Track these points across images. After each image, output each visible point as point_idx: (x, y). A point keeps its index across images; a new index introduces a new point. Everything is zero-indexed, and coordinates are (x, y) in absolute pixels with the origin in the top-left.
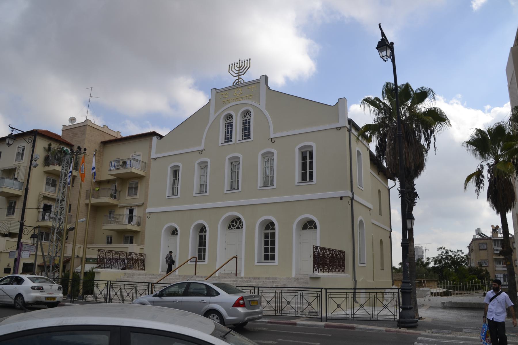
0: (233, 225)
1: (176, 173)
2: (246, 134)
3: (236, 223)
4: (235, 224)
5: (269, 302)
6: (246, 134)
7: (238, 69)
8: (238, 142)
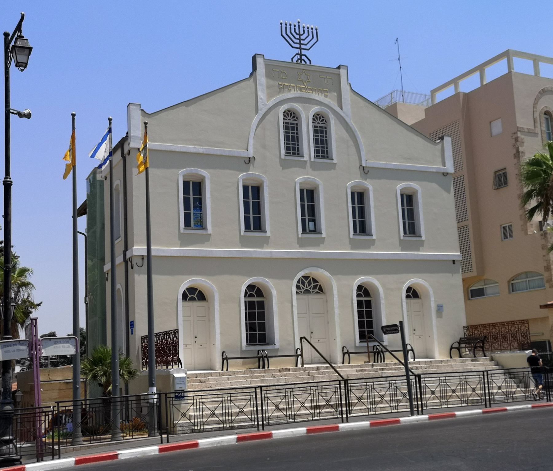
5: (474, 390)
7: (297, 37)
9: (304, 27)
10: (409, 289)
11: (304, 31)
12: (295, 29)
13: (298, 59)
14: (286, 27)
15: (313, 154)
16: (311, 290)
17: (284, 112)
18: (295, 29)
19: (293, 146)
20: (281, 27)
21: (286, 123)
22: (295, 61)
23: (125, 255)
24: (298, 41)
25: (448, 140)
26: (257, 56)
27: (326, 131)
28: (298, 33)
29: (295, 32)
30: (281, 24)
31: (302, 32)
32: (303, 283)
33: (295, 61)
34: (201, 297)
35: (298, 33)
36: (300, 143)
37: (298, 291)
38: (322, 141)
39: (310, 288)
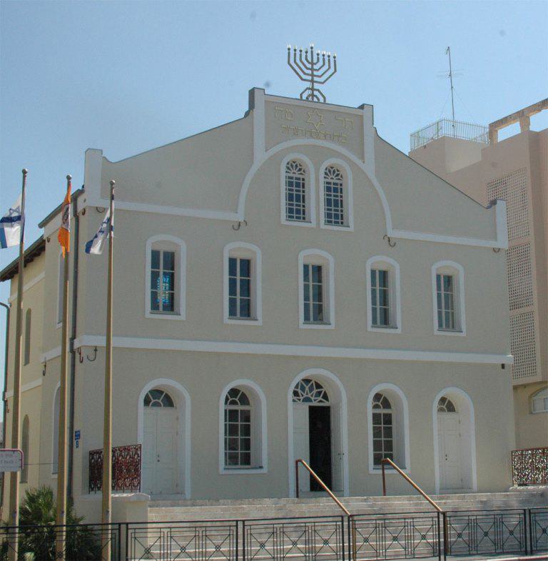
2: (335, 213)
6: (335, 213)
7: (309, 66)
9: (318, 54)
10: (443, 400)
11: (318, 58)
12: (306, 56)
13: (309, 96)
14: (295, 54)
15: (323, 218)
16: (313, 398)
17: (288, 163)
18: (306, 56)
19: (296, 207)
20: (289, 53)
21: (290, 178)
22: (304, 98)
23: (72, 345)
24: (310, 72)
25: (501, 205)
26: (256, 90)
27: (341, 189)
28: (310, 61)
29: (306, 59)
30: (289, 49)
31: (315, 61)
32: (303, 389)
33: (304, 98)
34: (169, 402)
35: (310, 60)
36: (306, 204)
37: (295, 398)
38: (336, 202)
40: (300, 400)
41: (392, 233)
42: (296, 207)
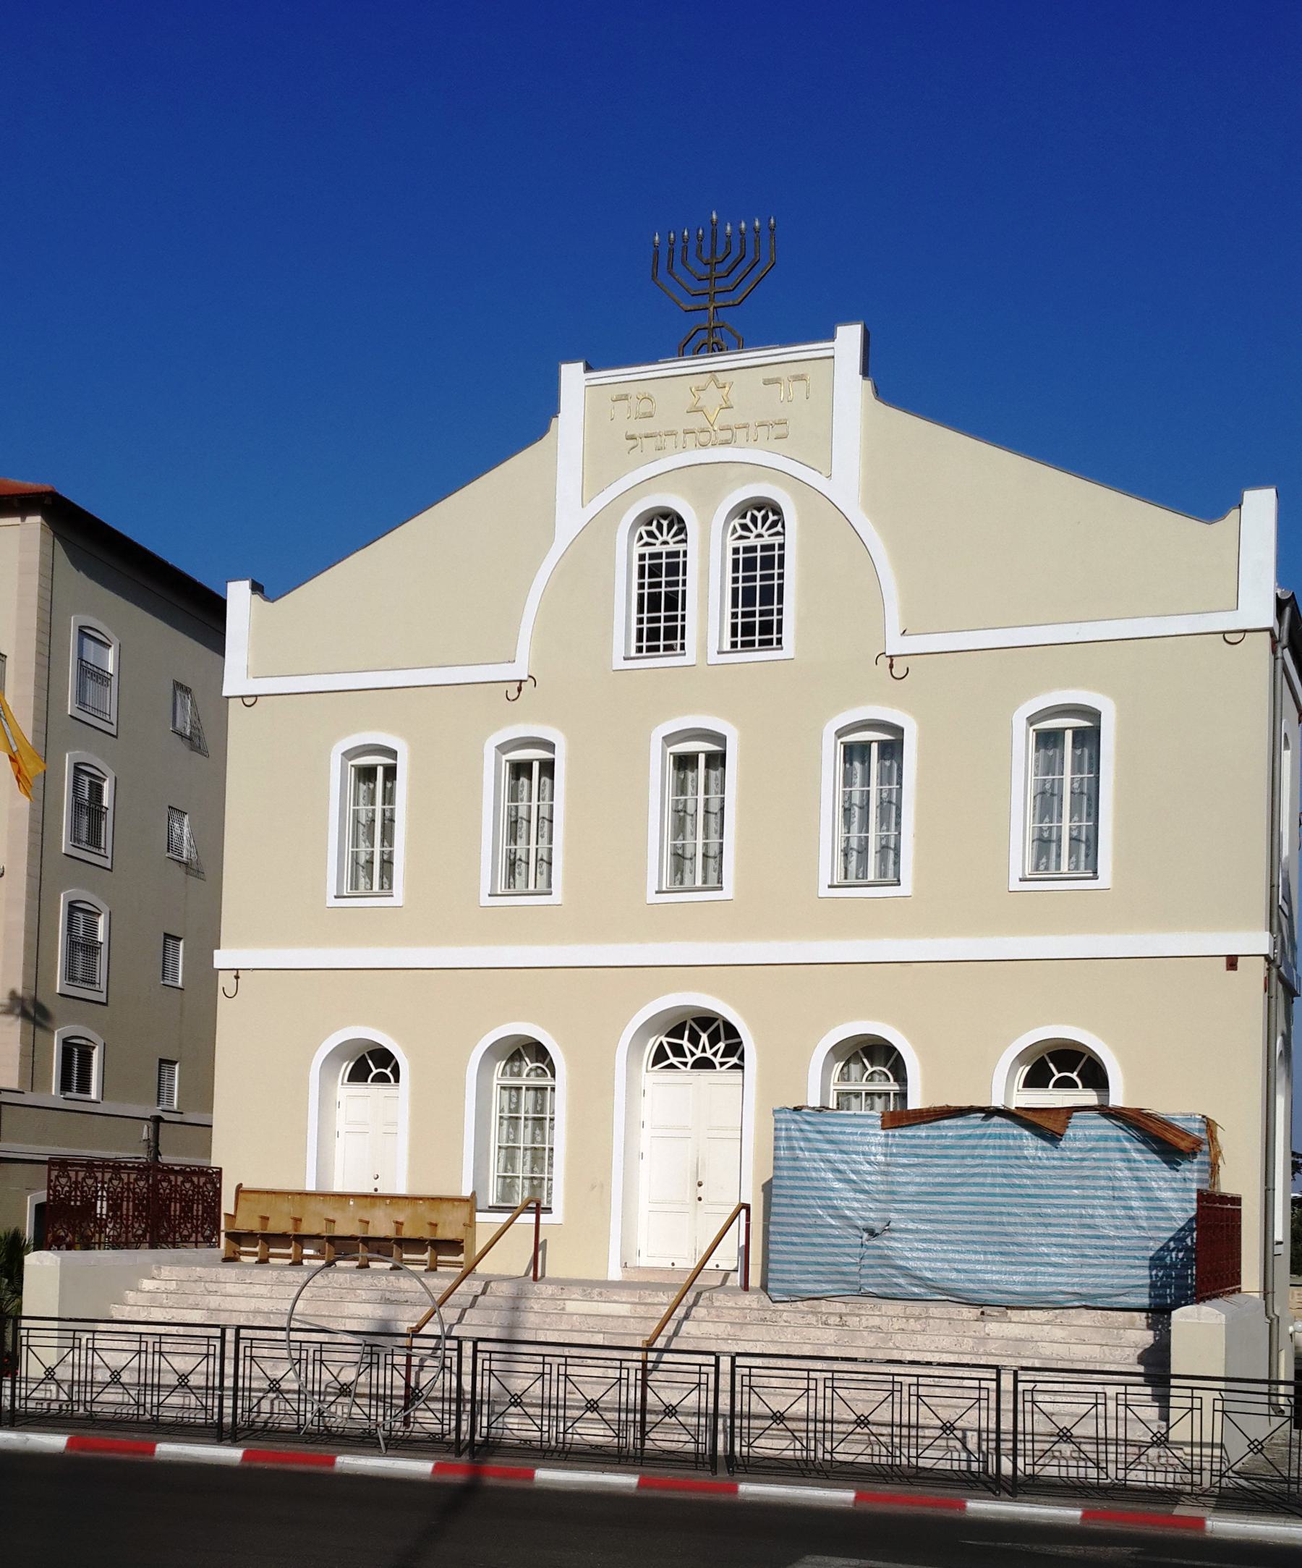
0: (678, 1051)
1: (375, 775)
2: (757, 619)
3: (695, 1040)
4: (686, 1043)
6: (757, 619)
8: (714, 658)
16: (717, 1060)
19: (661, 617)
39: (715, 1054)
40: (685, 1064)
41: (895, 645)
42: (661, 617)
